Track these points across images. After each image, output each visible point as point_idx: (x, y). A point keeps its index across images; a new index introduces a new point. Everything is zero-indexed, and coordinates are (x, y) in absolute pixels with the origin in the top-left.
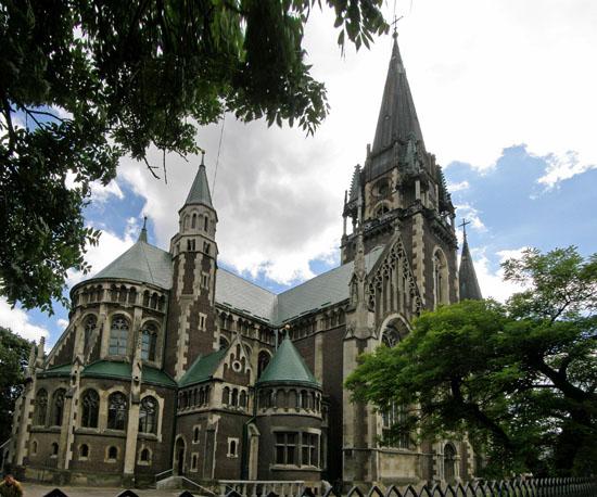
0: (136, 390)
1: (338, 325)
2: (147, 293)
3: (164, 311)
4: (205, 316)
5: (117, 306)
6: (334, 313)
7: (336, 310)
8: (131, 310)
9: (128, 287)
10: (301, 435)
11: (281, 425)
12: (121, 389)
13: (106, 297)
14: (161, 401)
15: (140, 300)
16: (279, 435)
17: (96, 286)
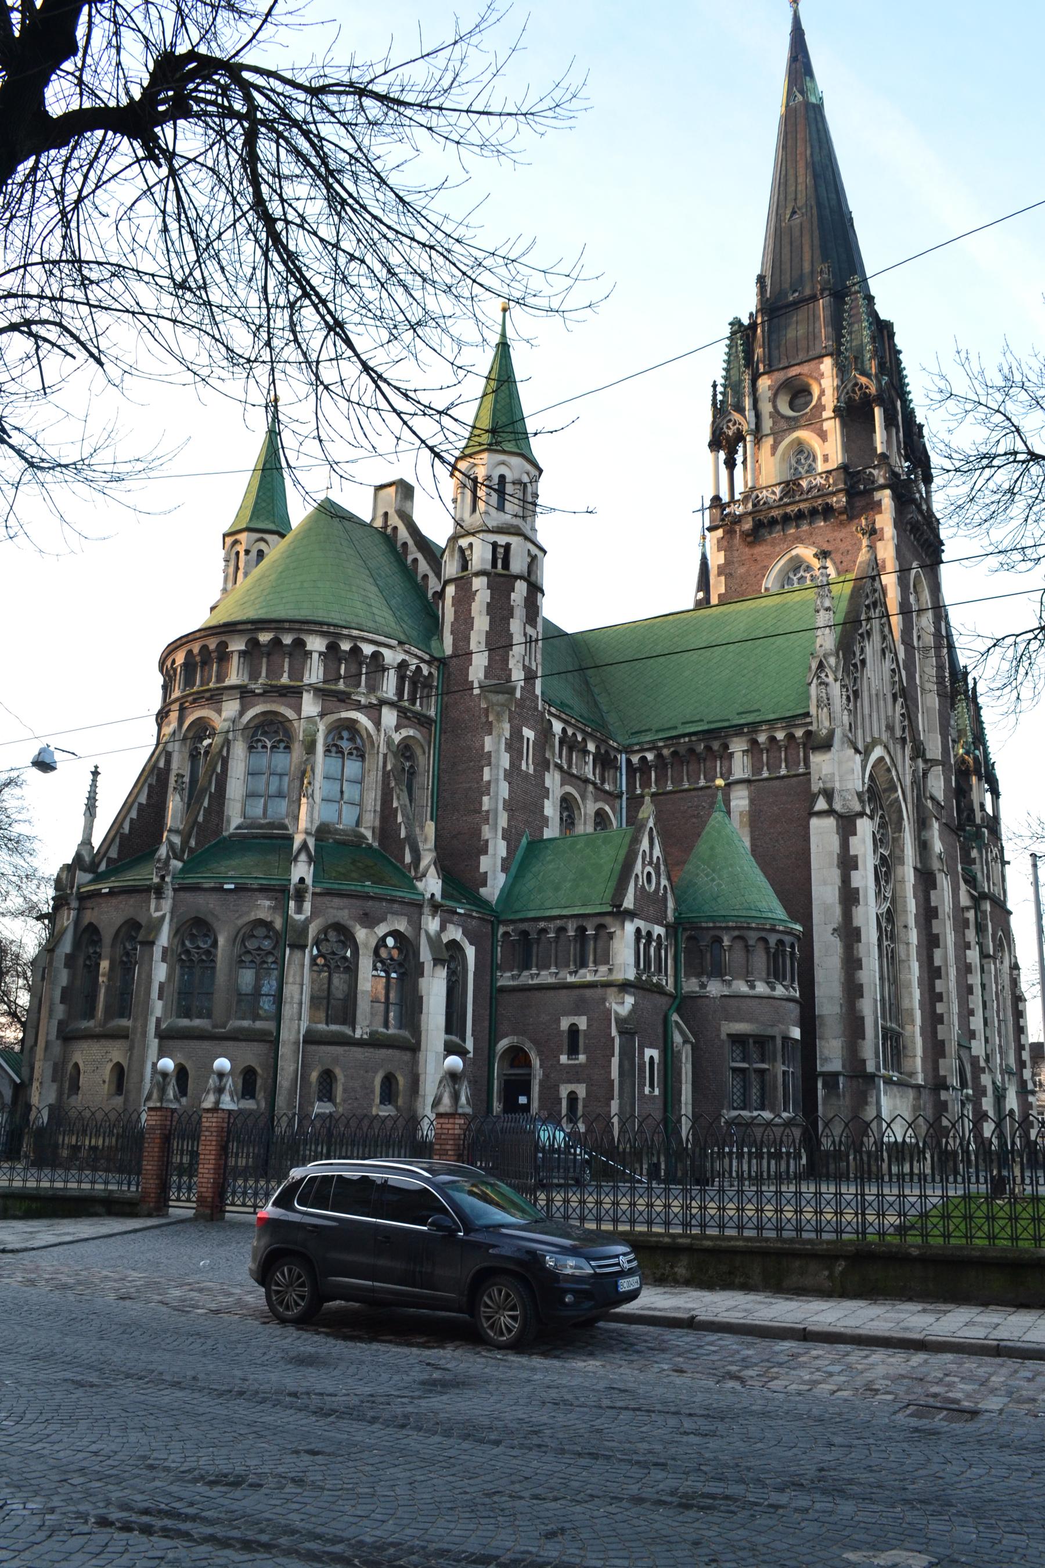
0: (432, 924)
1: (783, 772)
2: (403, 666)
3: (432, 713)
5: (344, 699)
6: (772, 739)
7: (780, 735)
8: (374, 710)
9: (368, 649)
10: (779, 1042)
11: (741, 1020)
12: (402, 925)
13: (315, 673)
14: (470, 952)
15: (389, 686)
16: (738, 1039)
17: (287, 640)
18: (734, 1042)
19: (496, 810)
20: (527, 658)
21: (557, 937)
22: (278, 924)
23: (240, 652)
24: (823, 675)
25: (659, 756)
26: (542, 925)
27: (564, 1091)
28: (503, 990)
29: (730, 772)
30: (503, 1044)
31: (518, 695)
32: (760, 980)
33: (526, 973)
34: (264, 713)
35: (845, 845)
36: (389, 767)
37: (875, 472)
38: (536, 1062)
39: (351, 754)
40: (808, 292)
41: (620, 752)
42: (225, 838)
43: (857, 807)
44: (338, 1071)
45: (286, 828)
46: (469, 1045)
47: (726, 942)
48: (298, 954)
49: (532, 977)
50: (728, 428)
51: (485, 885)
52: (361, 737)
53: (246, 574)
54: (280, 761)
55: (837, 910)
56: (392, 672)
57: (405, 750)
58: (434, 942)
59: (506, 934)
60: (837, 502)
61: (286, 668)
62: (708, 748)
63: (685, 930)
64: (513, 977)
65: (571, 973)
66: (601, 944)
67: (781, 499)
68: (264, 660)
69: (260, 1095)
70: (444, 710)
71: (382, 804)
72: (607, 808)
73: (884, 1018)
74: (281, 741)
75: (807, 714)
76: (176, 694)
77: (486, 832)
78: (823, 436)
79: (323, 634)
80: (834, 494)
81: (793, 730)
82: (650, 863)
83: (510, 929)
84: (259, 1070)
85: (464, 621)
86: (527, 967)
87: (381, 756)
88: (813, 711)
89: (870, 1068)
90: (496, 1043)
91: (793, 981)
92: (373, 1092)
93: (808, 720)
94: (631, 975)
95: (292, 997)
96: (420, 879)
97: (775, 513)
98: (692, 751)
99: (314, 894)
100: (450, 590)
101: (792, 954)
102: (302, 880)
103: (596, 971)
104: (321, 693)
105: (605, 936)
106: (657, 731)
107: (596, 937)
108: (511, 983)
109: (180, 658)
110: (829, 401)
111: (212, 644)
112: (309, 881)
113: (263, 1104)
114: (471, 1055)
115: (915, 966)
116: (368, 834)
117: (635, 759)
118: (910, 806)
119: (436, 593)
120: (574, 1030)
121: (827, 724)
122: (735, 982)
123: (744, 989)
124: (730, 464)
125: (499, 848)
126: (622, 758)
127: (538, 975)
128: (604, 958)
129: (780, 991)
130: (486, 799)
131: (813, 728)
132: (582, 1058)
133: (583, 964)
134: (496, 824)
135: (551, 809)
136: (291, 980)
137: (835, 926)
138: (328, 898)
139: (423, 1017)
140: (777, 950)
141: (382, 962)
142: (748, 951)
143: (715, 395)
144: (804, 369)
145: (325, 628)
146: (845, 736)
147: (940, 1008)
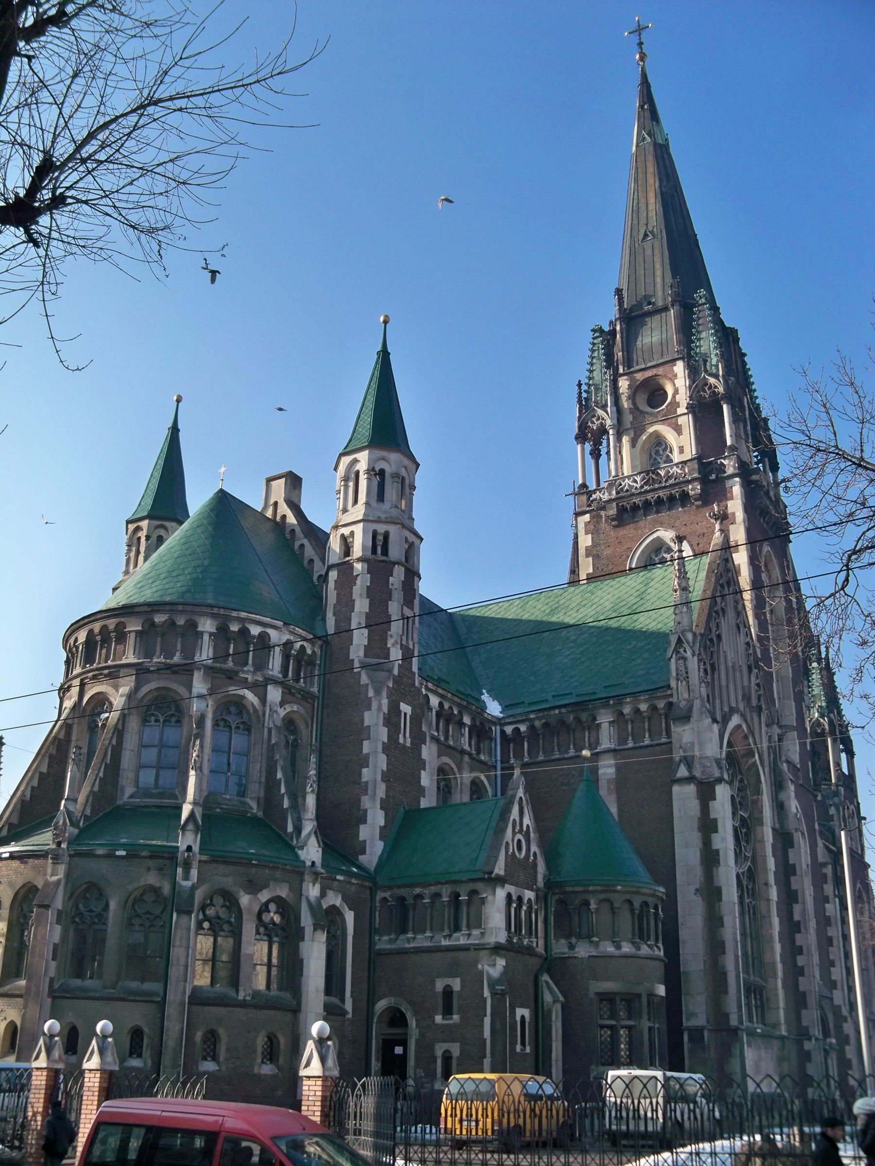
0: (313, 891)
1: (647, 742)
2: (288, 645)
3: (315, 689)
4: (409, 712)
5: (231, 676)
6: (637, 711)
7: (643, 707)
8: (260, 689)
9: (255, 630)
10: (644, 999)
11: (609, 979)
12: (283, 892)
13: (205, 653)
14: (350, 917)
16: (606, 998)
17: (181, 621)
18: (601, 1000)
19: (375, 780)
20: (404, 638)
21: (432, 903)
22: (166, 889)
23: (136, 632)
24: (682, 650)
25: (532, 728)
26: (418, 890)
27: (439, 1050)
28: (380, 953)
29: (598, 742)
30: (381, 1005)
31: (396, 672)
32: (625, 940)
33: (402, 937)
34: (157, 689)
35: (705, 809)
36: (273, 741)
37: (725, 462)
38: (412, 1023)
39: (238, 728)
40: (660, 303)
41: (495, 724)
42: (119, 807)
43: (717, 773)
44: (221, 1032)
45: (176, 798)
46: (349, 1006)
47: (593, 906)
48: (185, 918)
49: (408, 941)
50: (593, 422)
51: (363, 852)
52: (248, 712)
53: (146, 559)
54: (172, 734)
55: (699, 872)
56: (277, 649)
57: (289, 723)
58: (314, 909)
59: (385, 899)
60: (692, 490)
61: (179, 647)
62: (578, 720)
63: (554, 894)
64: (390, 941)
65: (445, 937)
66: (473, 909)
67: (642, 487)
68: (159, 639)
69: (147, 1053)
70: (325, 687)
71: (267, 777)
72: (483, 778)
73: (746, 971)
74: (173, 715)
75: (669, 687)
76: (78, 670)
77: (366, 802)
78: (678, 430)
79: (214, 616)
80: (688, 482)
81: (656, 702)
82: (521, 831)
83: (387, 895)
84: (146, 1030)
85: (346, 604)
86: (404, 931)
87: (266, 730)
88: (673, 684)
89: (734, 1021)
90: (374, 1004)
91: (657, 940)
92: (255, 1051)
93: (669, 692)
94: (502, 937)
95: (178, 960)
96: (302, 848)
97: (637, 500)
98: (562, 722)
99: (200, 861)
100: (333, 575)
101: (656, 914)
102: (189, 848)
103: (469, 935)
104: (210, 671)
105: (476, 900)
106: (530, 704)
107: (469, 903)
108: (388, 946)
109: (82, 636)
110: (683, 399)
111: (112, 623)
112: (196, 848)
113: (149, 1062)
114: (350, 1016)
115: (776, 921)
116: (254, 805)
117: (509, 729)
118: (767, 770)
119: (321, 576)
120: (448, 993)
121: (686, 696)
122: (602, 943)
123: (611, 949)
124: (596, 454)
125: (377, 818)
126: (496, 730)
127: (414, 938)
128: (477, 922)
129: (645, 950)
130: (365, 771)
131: (674, 699)
132: (456, 1017)
133: (457, 928)
134: (375, 794)
135: (426, 779)
136: (177, 943)
137: (698, 886)
138: (215, 865)
139: (304, 979)
140: (641, 911)
141: (265, 926)
142: (613, 913)
143: (580, 393)
144: (660, 371)
145: (216, 610)
146: (703, 706)
147: (801, 961)
